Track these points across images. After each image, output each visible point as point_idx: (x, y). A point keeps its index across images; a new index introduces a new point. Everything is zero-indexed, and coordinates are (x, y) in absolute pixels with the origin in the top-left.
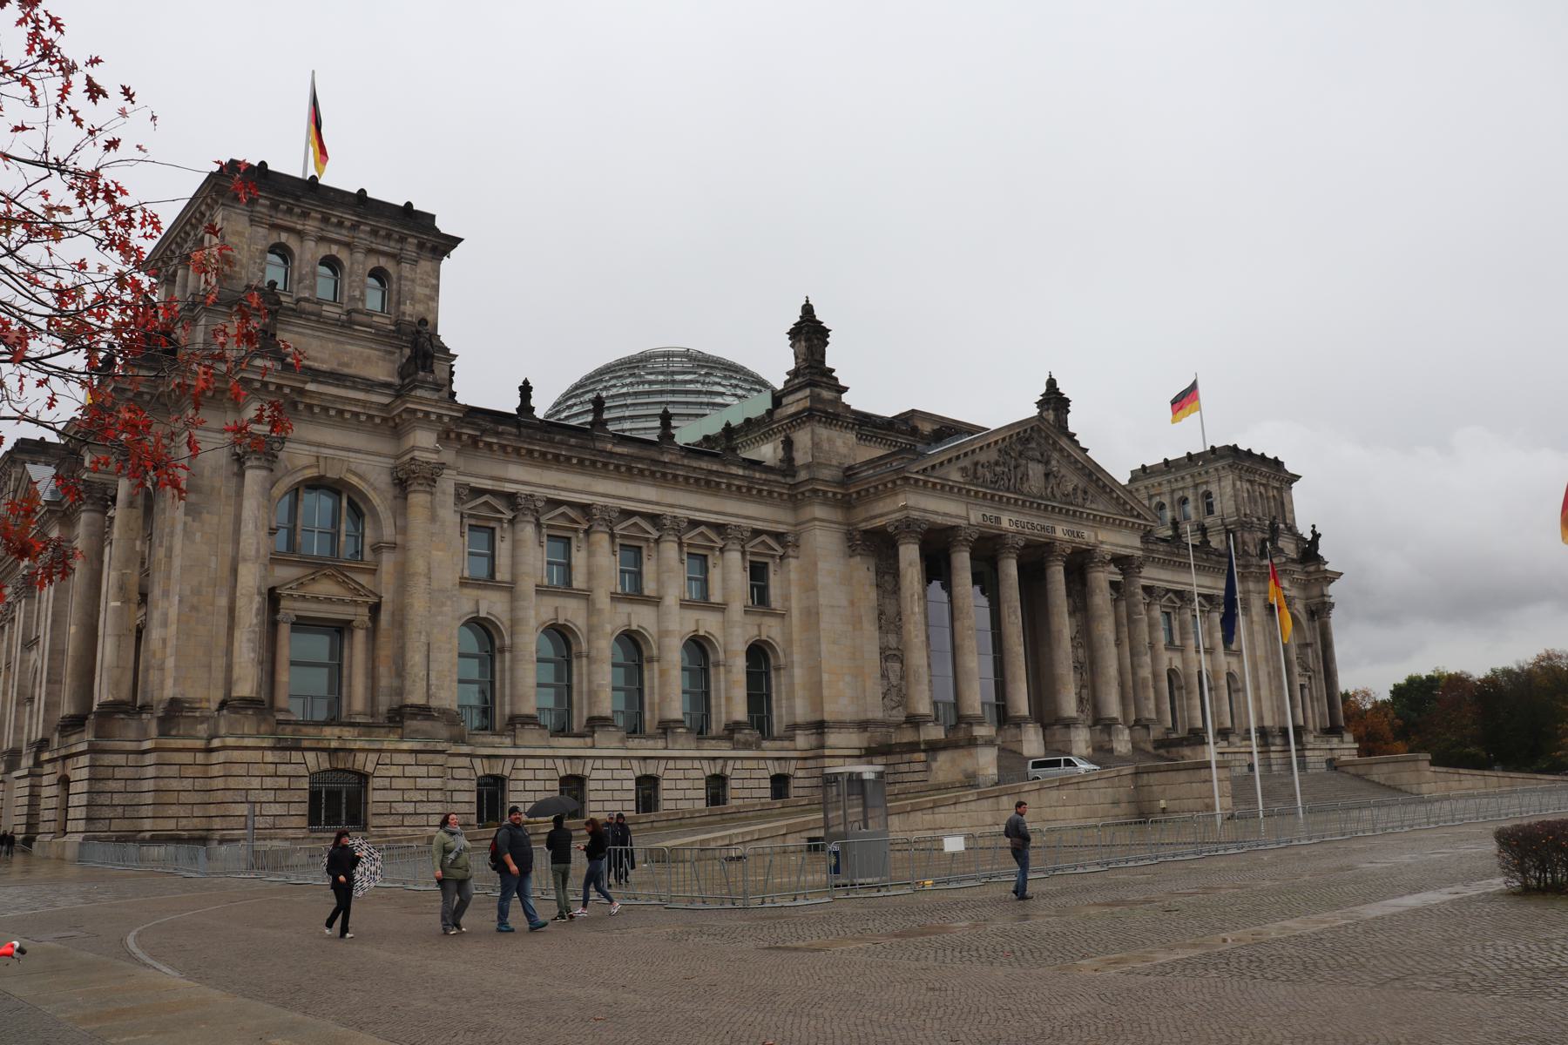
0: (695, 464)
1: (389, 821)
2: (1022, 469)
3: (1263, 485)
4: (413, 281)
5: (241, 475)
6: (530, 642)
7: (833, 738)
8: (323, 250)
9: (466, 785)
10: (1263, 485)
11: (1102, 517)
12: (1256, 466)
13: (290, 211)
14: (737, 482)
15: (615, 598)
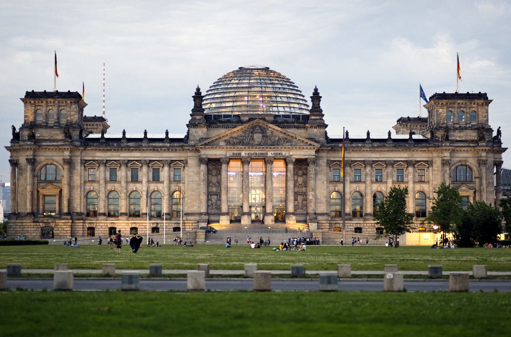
0: (154, 144)
1: (58, 237)
2: (249, 137)
3: (465, 107)
4: (70, 111)
5: (27, 167)
6: (102, 196)
7: (190, 218)
8: (48, 108)
9: (82, 229)
10: (465, 107)
11: (289, 148)
12: (454, 101)
13: (38, 102)
14: (163, 149)
15: (127, 182)
